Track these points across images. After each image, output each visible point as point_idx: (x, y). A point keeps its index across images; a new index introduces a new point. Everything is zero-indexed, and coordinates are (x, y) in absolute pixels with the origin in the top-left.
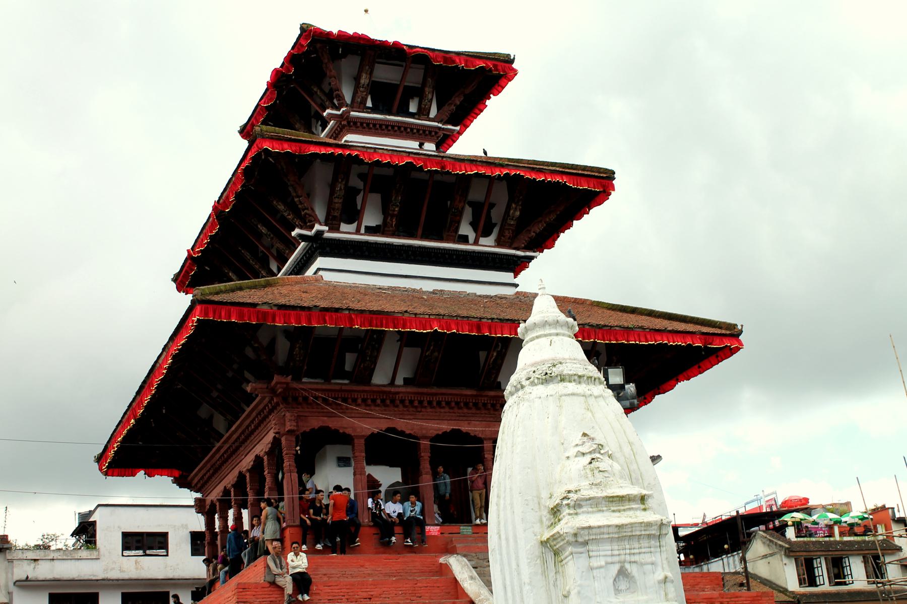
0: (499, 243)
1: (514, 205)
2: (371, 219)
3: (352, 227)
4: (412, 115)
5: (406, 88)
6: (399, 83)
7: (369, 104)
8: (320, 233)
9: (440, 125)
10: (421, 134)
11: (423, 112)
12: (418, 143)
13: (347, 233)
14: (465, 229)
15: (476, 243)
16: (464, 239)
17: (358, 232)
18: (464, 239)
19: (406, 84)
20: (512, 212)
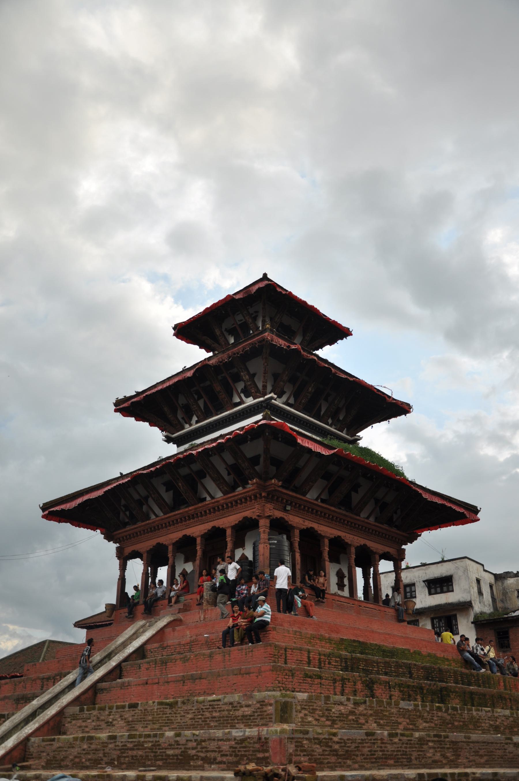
0: (254, 399)
3: (187, 426)
20: (244, 377)
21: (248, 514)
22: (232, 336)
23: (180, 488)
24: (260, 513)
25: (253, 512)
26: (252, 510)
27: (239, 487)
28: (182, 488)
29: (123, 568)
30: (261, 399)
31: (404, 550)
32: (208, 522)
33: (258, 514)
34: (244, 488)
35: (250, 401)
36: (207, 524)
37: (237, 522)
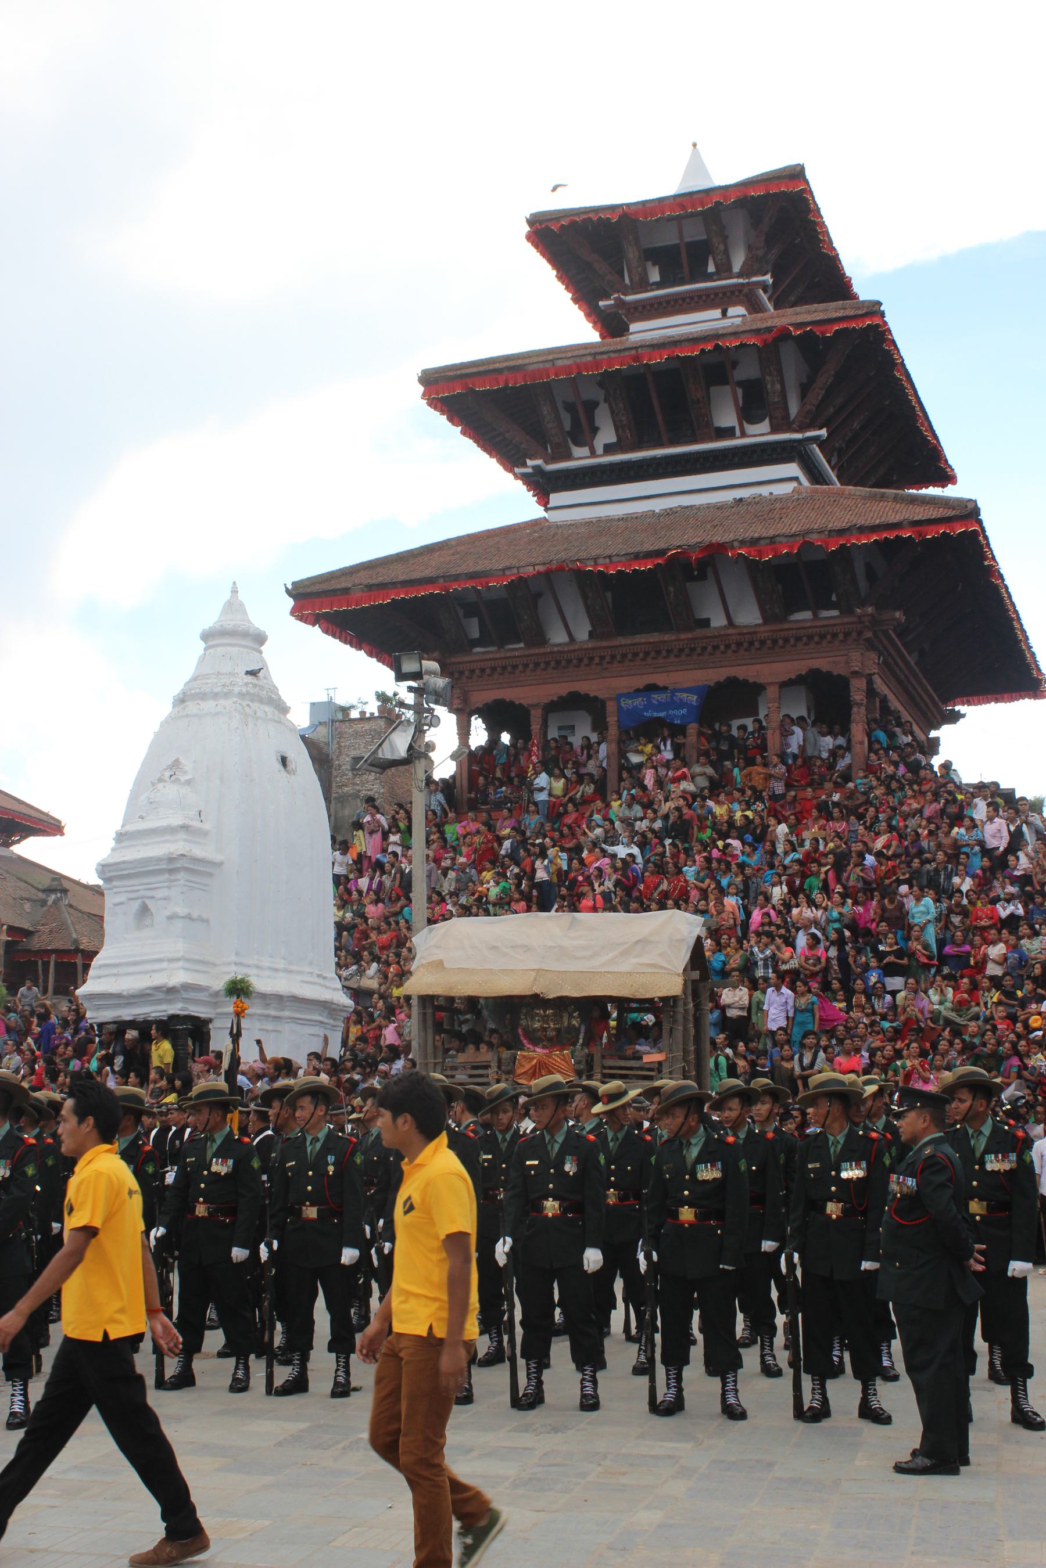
0: (774, 430)
1: (768, 378)
2: (607, 435)
3: (583, 451)
4: (709, 277)
5: (691, 246)
6: (678, 242)
7: (655, 276)
8: (537, 469)
9: (741, 281)
10: (721, 299)
11: (724, 269)
12: (720, 311)
13: (581, 458)
14: (727, 418)
15: (744, 434)
16: (727, 433)
17: (593, 454)
18: (727, 433)
19: (687, 240)
20: (769, 386)
21: (822, 664)
22: (654, 264)
25: (834, 662)
31: (936, 742)
35: (760, 433)
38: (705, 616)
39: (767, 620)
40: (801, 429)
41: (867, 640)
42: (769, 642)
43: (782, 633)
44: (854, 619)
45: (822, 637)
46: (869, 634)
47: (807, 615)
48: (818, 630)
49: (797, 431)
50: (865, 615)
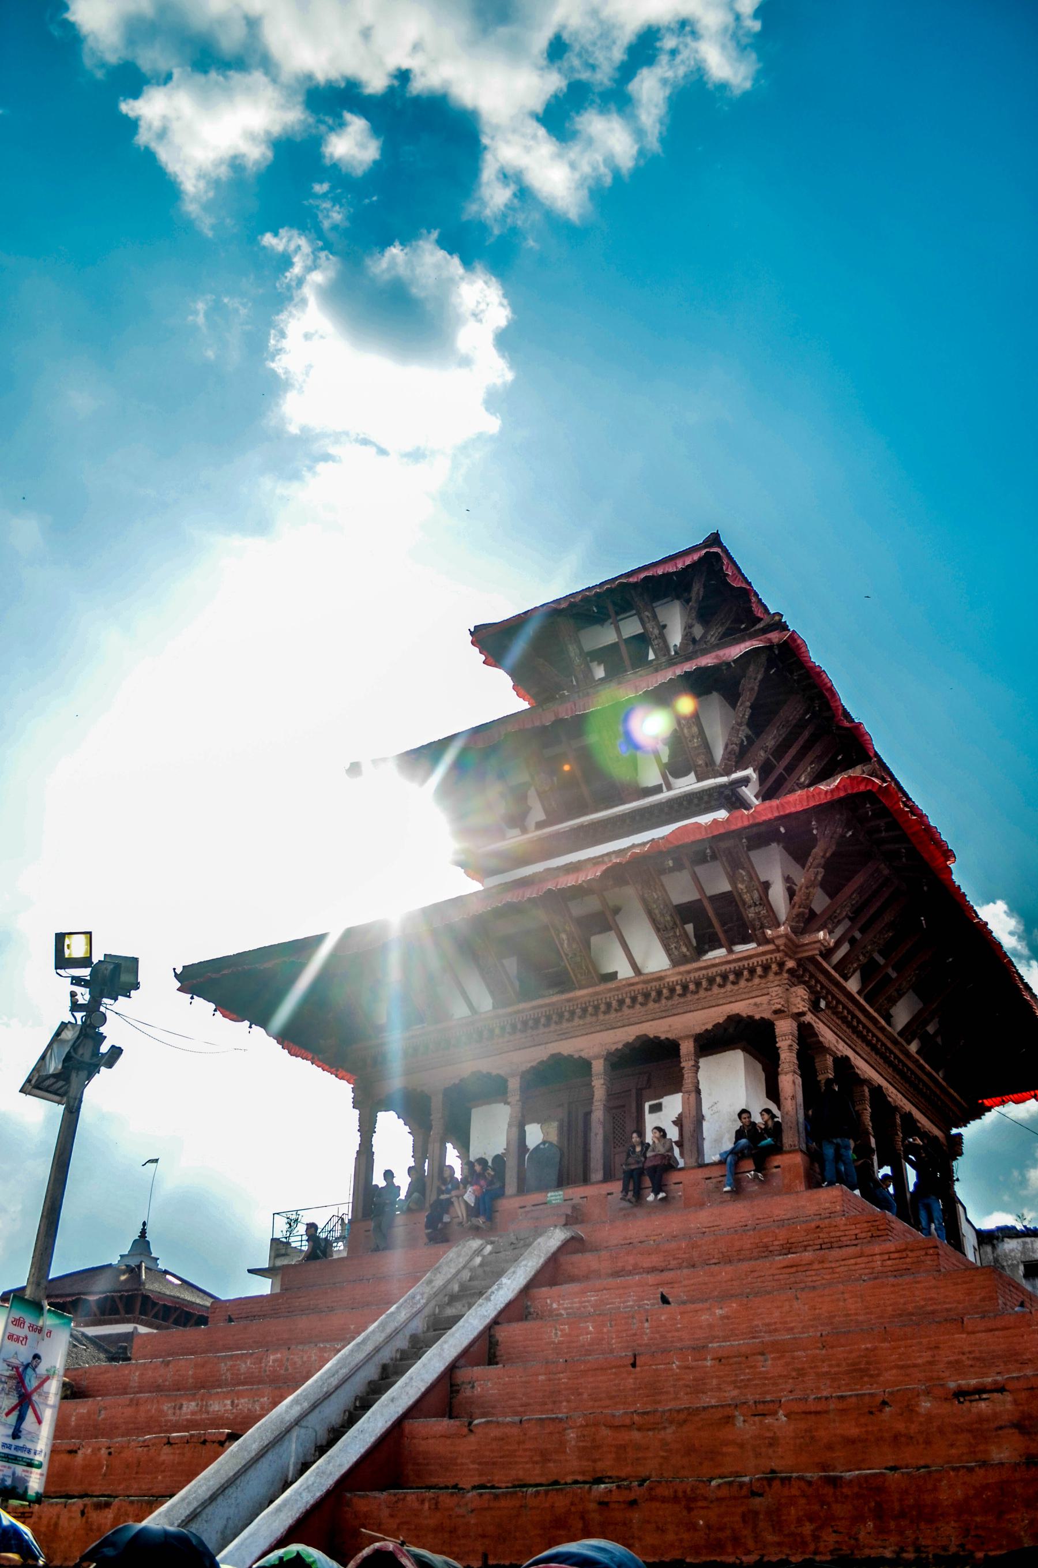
0: (699, 779)
21: (742, 1008)
22: (599, 664)
23: (562, 945)
24: (783, 1006)
25: (755, 1004)
26: (752, 1001)
27: (721, 946)
28: (565, 945)
29: (367, 1129)
30: (723, 780)
32: (624, 1026)
33: (779, 1006)
34: (730, 951)
36: (622, 1029)
37: (709, 1027)
38: (611, 970)
39: (675, 963)
40: (728, 773)
41: (790, 971)
42: (678, 988)
43: (692, 975)
44: (771, 947)
45: (738, 974)
46: (790, 964)
47: (721, 952)
48: (732, 966)
49: (722, 776)
50: (779, 937)
